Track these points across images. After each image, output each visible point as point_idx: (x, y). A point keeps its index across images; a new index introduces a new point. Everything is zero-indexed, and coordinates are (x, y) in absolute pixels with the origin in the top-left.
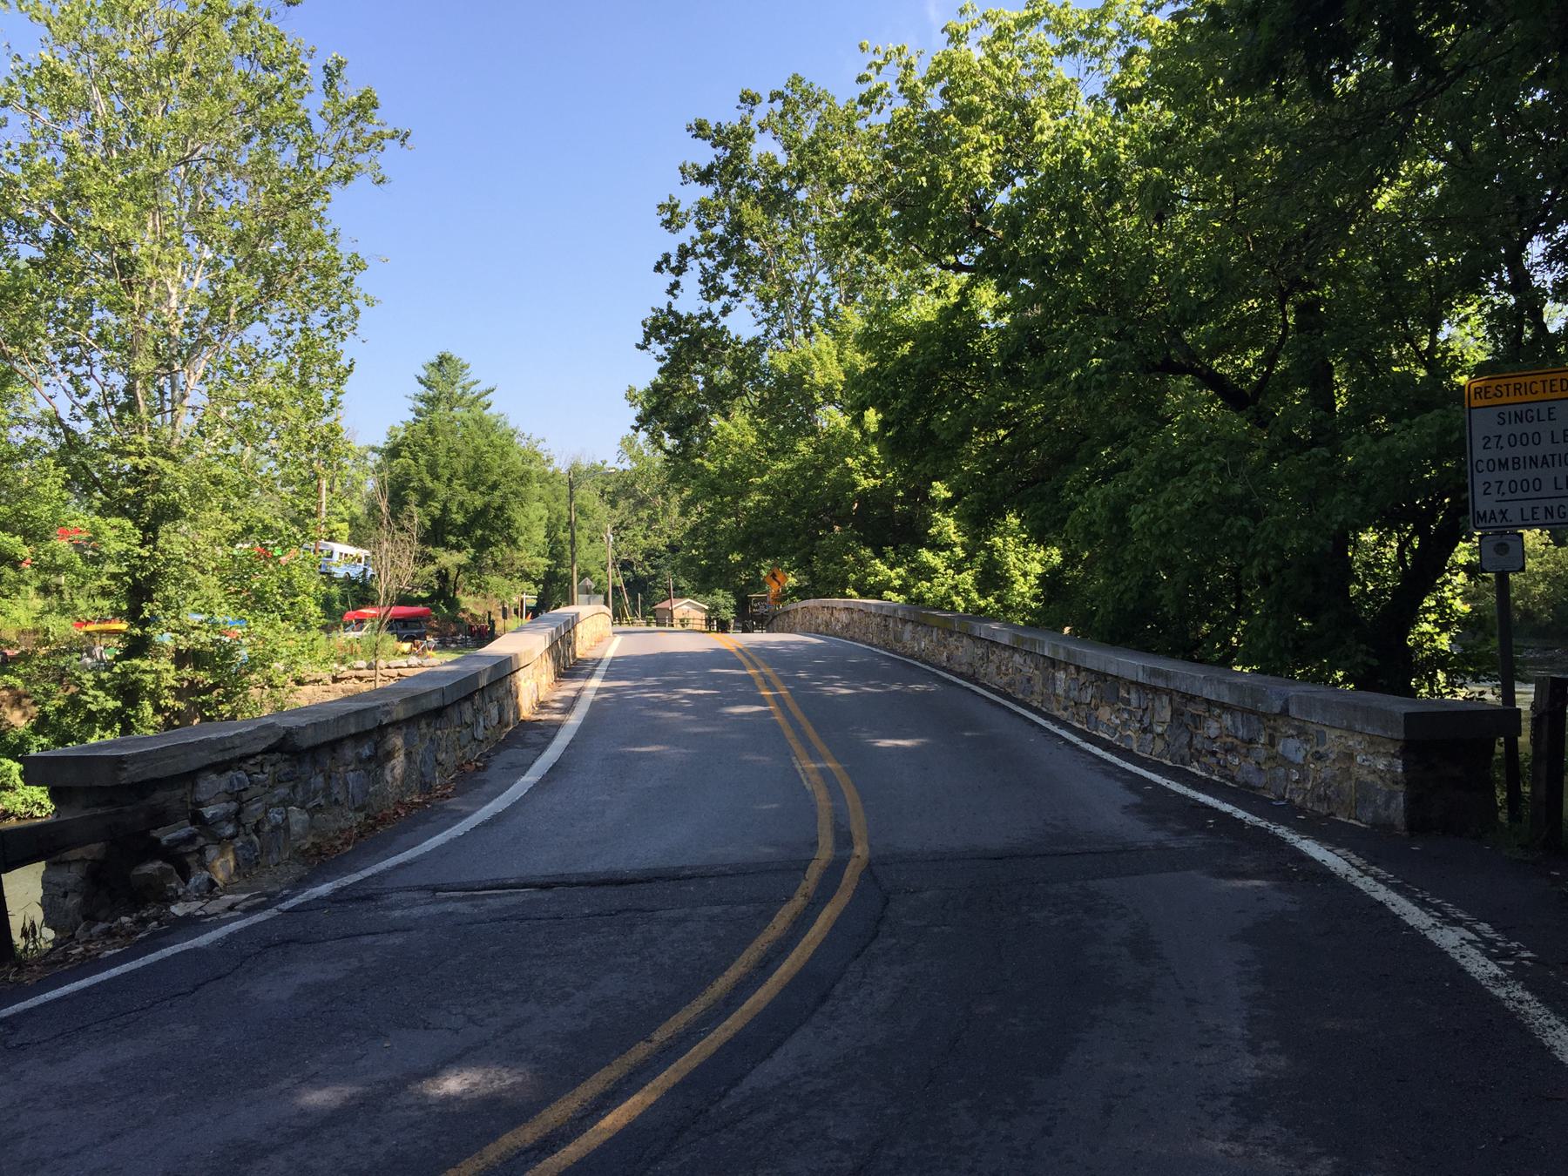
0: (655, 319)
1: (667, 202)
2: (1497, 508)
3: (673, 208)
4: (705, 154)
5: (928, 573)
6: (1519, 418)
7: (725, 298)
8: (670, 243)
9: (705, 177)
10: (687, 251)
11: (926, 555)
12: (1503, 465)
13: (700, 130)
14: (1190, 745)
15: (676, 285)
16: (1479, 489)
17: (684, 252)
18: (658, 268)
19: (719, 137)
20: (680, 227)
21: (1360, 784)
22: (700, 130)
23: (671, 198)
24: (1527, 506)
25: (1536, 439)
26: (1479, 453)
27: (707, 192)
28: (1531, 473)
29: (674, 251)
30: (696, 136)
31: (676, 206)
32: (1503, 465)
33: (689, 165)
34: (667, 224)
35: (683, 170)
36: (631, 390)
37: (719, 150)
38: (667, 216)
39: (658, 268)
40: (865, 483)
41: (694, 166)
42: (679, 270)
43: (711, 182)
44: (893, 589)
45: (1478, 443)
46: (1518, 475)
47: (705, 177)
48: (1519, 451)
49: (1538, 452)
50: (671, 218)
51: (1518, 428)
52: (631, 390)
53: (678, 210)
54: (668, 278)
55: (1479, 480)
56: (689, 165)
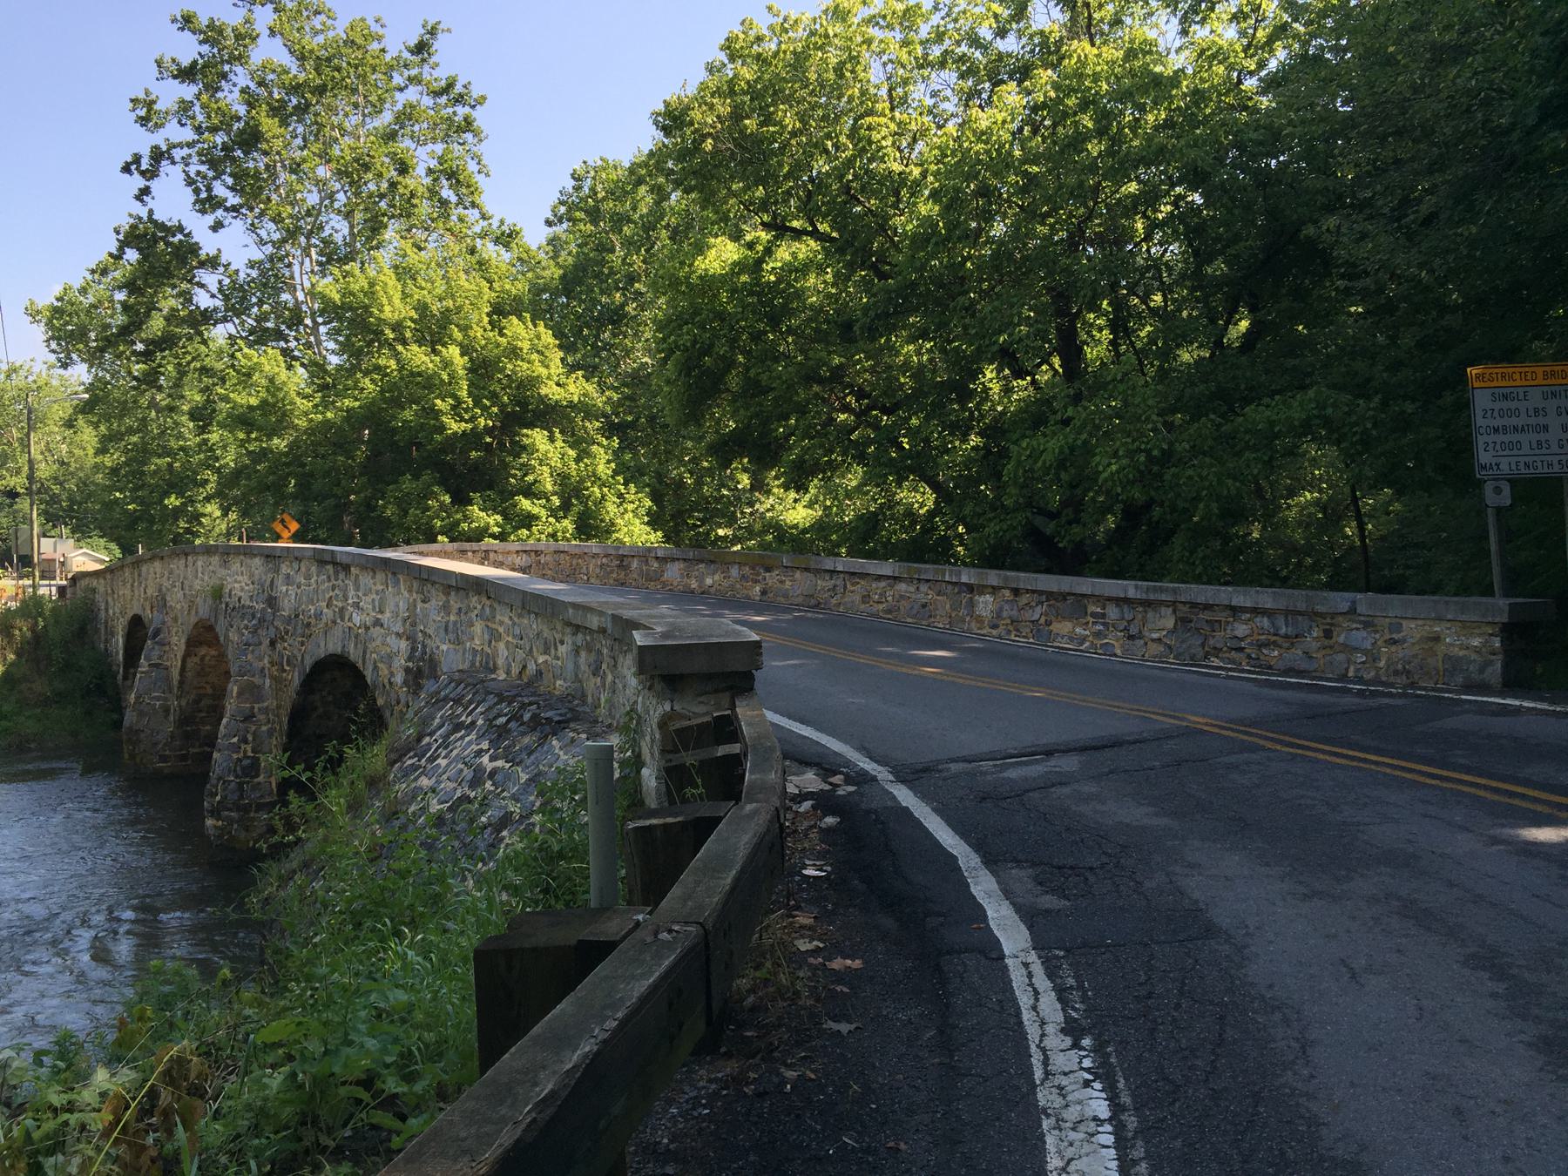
0: (133, 227)
1: (142, 96)
3: (150, 104)
4: (188, 49)
5: (528, 520)
6: (1505, 397)
7: (220, 213)
8: (143, 141)
9: (186, 74)
10: (162, 154)
11: (525, 504)
12: (1496, 430)
13: (187, 21)
14: (1203, 645)
15: (145, 191)
16: (1481, 446)
17: (158, 155)
18: (126, 169)
19: (212, 34)
20: (162, 126)
21: (1447, 658)
22: (187, 21)
26: (1480, 421)
27: (188, 91)
28: (1515, 437)
29: (146, 153)
30: (182, 29)
31: (153, 102)
32: (1496, 430)
34: (143, 121)
35: (159, 63)
37: (205, 49)
38: (143, 113)
39: (126, 169)
40: (454, 427)
41: (173, 60)
42: (150, 174)
43: (193, 81)
44: (493, 536)
46: (1506, 438)
47: (186, 74)
48: (1506, 421)
51: (1505, 405)
53: (155, 107)
54: (138, 182)
55: (1481, 440)
56: (167, 59)
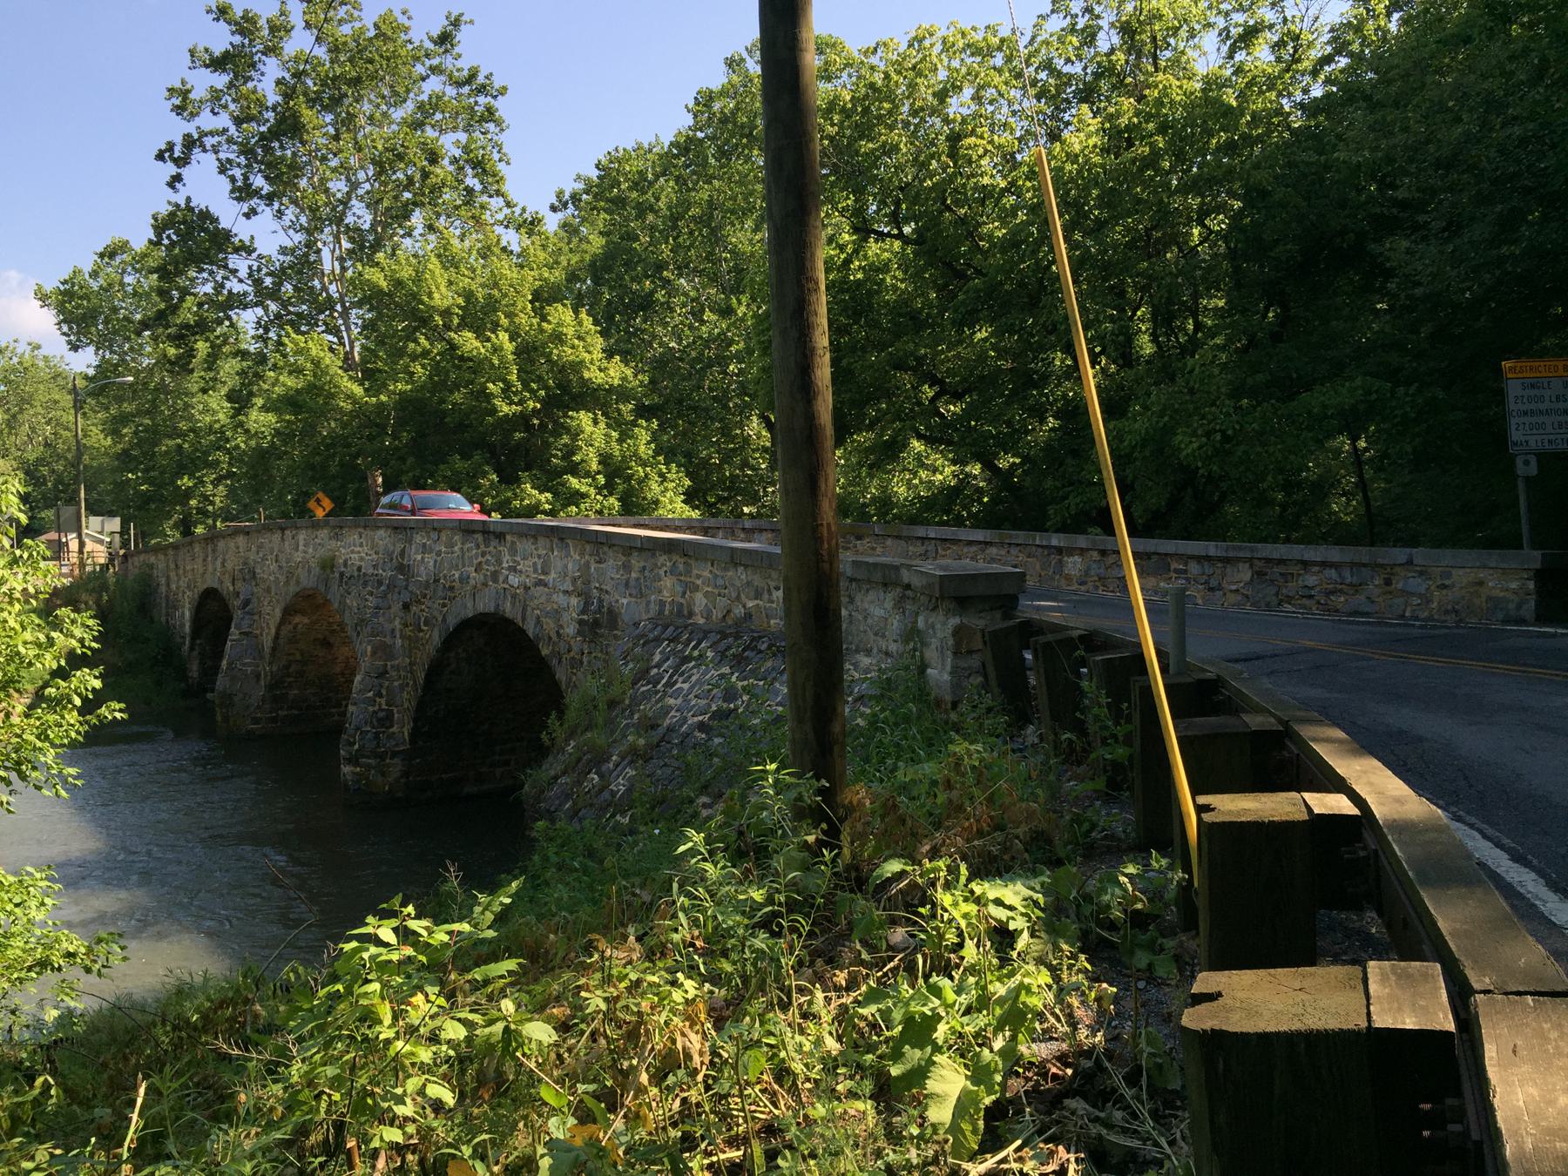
0: (172, 214)
1: (178, 85)
2: (1523, 439)
3: (184, 94)
4: (221, 39)
5: (576, 497)
6: (1533, 386)
7: (254, 202)
8: (177, 129)
9: (218, 63)
10: (194, 142)
11: (574, 482)
12: (1525, 413)
13: (222, 12)
14: (1277, 594)
15: (177, 178)
16: (1513, 427)
17: (190, 143)
18: (160, 157)
19: (245, 26)
20: (198, 114)
21: (1489, 598)
22: (222, 12)
23: (183, 82)
24: (1539, 438)
25: (1541, 399)
26: (1512, 406)
27: (221, 80)
28: (1540, 419)
29: (178, 140)
30: (218, 19)
31: (189, 91)
32: (1525, 413)
33: (201, 48)
34: (179, 110)
35: (192, 53)
36: (40, 287)
37: (237, 39)
38: (177, 102)
39: (160, 157)
40: (505, 409)
41: (206, 50)
42: (182, 162)
43: (224, 70)
44: (544, 512)
45: (1512, 400)
46: (1534, 420)
47: (218, 63)
48: (1533, 406)
49: (1542, 407)
50: (183, 104)
51: (1533, 392)
52: (40, 287)
53: (191, 96)
54: (171, 169)
55: (1513, 421)
56: (201, 48)
